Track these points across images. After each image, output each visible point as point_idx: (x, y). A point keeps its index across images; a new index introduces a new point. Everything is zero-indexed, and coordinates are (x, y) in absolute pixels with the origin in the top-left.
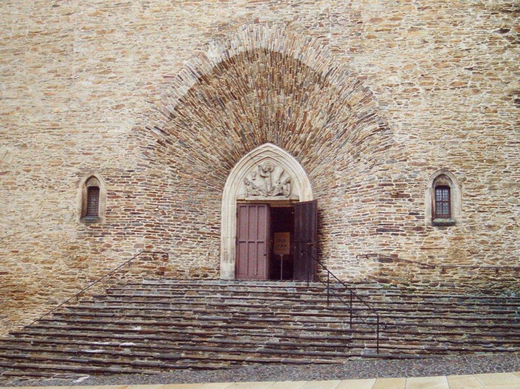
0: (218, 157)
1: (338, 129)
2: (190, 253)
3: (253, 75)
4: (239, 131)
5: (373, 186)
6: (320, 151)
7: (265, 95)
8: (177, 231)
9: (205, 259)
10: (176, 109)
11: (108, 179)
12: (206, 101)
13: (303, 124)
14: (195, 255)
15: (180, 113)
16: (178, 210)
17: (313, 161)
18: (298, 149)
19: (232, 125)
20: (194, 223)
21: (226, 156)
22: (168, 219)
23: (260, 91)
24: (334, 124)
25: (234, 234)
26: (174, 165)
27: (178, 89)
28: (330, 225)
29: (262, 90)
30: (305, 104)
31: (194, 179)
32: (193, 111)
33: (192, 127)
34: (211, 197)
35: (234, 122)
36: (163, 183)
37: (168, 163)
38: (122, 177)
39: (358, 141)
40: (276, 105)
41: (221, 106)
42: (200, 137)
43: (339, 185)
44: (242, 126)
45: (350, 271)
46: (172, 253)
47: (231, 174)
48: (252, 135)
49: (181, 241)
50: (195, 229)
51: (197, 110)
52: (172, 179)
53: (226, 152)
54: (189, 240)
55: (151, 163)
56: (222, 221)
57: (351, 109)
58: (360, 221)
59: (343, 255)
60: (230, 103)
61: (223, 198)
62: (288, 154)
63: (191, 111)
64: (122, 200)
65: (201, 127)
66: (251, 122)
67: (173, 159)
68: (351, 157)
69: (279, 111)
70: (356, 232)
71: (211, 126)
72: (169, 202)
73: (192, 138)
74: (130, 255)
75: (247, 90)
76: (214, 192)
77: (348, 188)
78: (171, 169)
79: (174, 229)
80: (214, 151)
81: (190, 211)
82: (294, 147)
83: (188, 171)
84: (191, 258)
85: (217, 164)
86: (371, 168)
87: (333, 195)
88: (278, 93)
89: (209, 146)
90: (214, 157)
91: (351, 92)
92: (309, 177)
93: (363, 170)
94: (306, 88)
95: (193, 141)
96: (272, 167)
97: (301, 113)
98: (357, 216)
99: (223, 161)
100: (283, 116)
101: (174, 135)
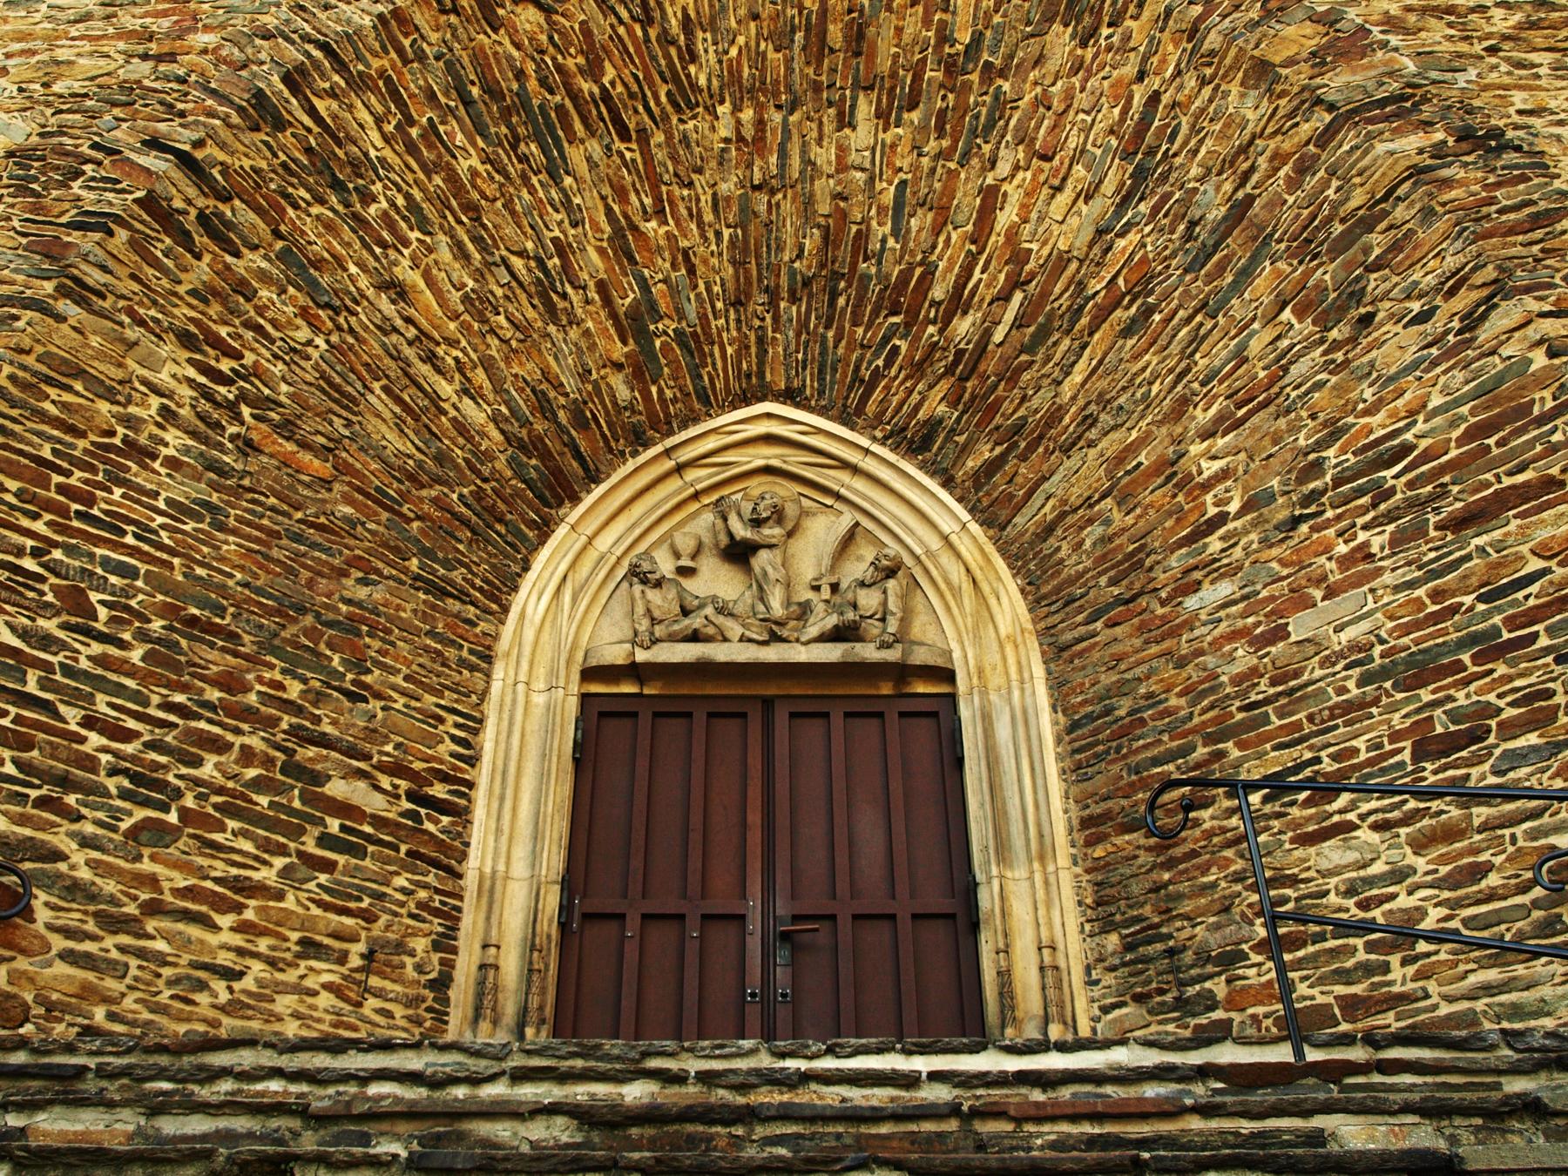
0: (495, 419)
1: (1195, 213)
2: (225, 921)
3: (722, 25)
4: (624, 303)
6: (1077, 377)
7: (773, 139)
8: (150, 746)
9: (328, 987)
10: (287, 79)
12: (467, 102)
13: (972, 259)
14: (263, 945)
15: (312, 112)
16: (193, 621)
17: (1031, 447)
18: (936, 405)
19: (592, 263)
20: (294, 731)
21: (539, 427)
22: (97, 648)
23: (747, 115)
24: (1166, 197)
25: (553, 861)
26: (225, 365)
28: (1201, 751)
29: (760, 108)
30: (986, 148)
31: (337, 486)
32: (389, 128)
33: (373, 209)
34: (425, 618)
35: (601, 251)
36: (121, 430)
37: (186, 340)
39: (1338, 228)
40: (823, 187)
41: (545, 150)
42: (405, 272)
43: (1233, 507)
44: (644, 286)
45: (1480, 1005)
46: (75, 890)
47: (562, 531)
48: (694, 343)
49: (173, 818)
50: (294, 769)
51: (414, 132)
52: (193, 434)
53: (543, 406)
54: (229, 832)
55: (62, 292)
56: (483, 775)
57: (1277, 79)
58: (1473, 639)
59: (1364, 905)
60: (595, 148)
61: (503, 645)
62: (876, 448)
63: (379, 121)
65: (423, 225)
66: (691, 271)
67: (223, 331)
68: (1307, 327)
69: (843, 216)
70: (1454, 716)
71: (477, 240)
72: (133, 551)
73: (361, 265)
75: (685, 98)
76: (453, 605)
77: (1307, 500)
78: (202, 379)
79: (131, 724)
80: (480, 376)
81: (274, 651)
82: (915, 397)
83: (307, 426)
84: (225, 959)
85: (489, 456)
86: (1472, 321)
87: (1197, 575)
88: (841, 115)
89: (453, 343)
90: (475, 414)
91: (1258, 24)
92: (1003, 552)
93: (1408, 358)
94: (998, 62)
95: (363, 282)
96: (791, 511)
97: (966, 201)
98: (1435, 618)
99: (522, 447)
100: (862, 237)
101: (258, 210)
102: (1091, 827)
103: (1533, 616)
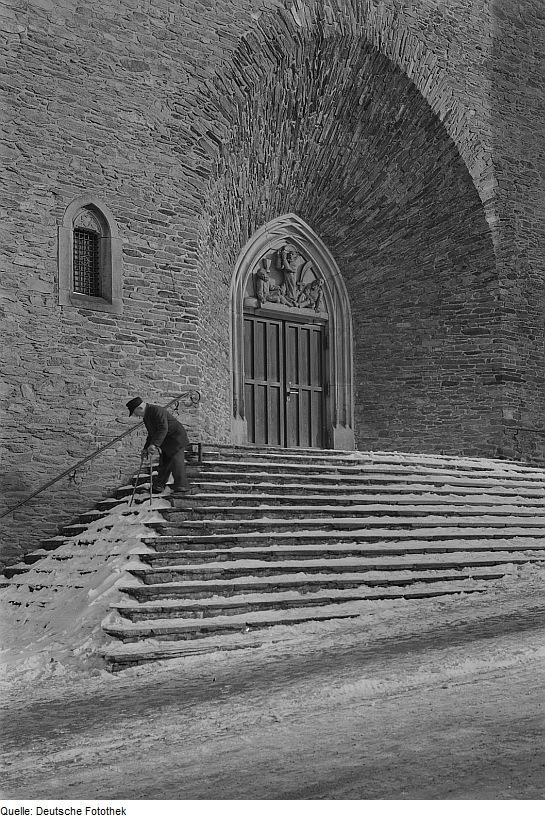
5: (489, 311)
11: (123, 221)
27: (244, 68)
38: (152, 221)
43: (416, 303)
64: (153, 271)
74: (176, 388)
86: (487, 281)
102: (359, 375)
103: (475, 361)
